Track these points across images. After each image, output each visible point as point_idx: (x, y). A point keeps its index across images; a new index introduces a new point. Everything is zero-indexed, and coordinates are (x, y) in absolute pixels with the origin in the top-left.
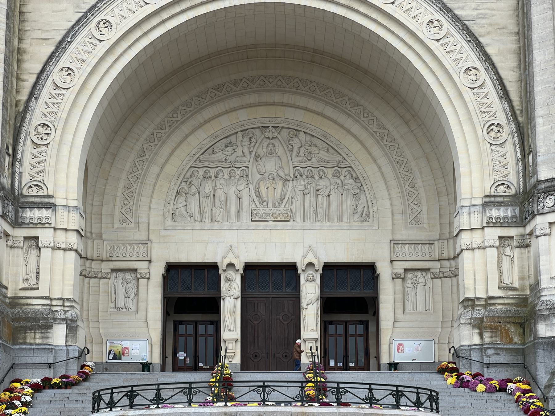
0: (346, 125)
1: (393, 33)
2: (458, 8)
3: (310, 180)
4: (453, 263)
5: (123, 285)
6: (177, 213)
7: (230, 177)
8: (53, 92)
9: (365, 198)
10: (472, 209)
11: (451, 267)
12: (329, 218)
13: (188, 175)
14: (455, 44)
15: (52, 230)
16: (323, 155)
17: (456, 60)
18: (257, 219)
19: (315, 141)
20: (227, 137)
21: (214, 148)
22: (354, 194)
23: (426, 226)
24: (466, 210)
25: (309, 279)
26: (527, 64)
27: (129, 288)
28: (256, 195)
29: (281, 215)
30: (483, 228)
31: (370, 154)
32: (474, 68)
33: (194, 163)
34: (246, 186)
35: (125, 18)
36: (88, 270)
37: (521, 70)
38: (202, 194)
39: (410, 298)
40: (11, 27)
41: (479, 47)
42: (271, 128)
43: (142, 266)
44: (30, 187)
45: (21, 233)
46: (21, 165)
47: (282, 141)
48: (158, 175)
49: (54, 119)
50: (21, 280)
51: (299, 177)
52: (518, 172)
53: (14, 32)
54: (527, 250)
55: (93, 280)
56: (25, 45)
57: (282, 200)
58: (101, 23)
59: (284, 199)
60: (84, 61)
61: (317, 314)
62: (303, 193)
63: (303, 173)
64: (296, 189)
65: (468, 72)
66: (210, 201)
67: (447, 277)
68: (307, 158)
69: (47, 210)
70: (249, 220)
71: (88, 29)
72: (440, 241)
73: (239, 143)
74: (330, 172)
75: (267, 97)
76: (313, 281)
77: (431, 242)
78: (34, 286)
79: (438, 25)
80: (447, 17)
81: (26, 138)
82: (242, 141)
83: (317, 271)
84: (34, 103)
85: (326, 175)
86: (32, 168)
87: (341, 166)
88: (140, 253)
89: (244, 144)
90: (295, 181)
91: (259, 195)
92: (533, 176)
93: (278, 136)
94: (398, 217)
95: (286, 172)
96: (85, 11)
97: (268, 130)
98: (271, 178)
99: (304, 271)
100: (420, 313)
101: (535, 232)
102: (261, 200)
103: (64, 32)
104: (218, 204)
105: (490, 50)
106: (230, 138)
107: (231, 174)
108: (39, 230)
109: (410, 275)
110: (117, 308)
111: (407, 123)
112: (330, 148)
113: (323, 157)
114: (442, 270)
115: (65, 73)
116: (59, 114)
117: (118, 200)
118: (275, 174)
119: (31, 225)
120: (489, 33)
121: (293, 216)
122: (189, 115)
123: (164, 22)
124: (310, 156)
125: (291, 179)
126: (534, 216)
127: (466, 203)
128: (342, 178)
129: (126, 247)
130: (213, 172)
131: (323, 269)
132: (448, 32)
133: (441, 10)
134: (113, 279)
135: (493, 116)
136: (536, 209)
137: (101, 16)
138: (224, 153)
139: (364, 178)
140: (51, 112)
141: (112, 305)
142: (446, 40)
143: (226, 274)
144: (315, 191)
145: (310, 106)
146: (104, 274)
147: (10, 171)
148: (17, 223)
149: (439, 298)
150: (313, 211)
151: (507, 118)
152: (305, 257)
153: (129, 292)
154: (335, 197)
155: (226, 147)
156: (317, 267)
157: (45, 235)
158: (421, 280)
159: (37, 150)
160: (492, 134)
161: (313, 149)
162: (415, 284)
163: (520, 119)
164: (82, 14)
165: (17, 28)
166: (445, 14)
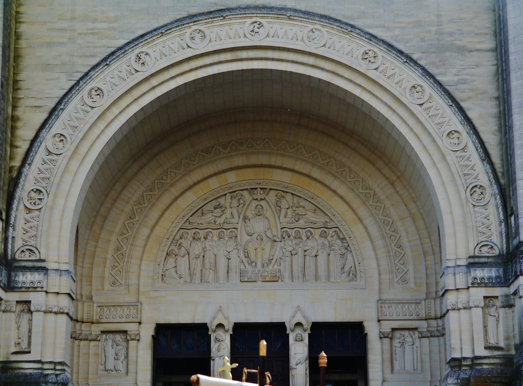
0: (333, 187)
1: (377, 97)
2: (440, 74)
3: (297, 241)
4: (440, 321)
5: (113, 347)
6: (167, 275)
7: (220, 238)
8: (46, 158)
9: (352, 258)
10: (457, 270)
11: (438, 326)
12: (317, 278)
13: (178, 237)
14: (437, 109)
15: (44, 293)
16: (311, 216)
17: (439, 124)
18: (246, 279)
19: (303, 203)
20: (215, 199)
21: (204, 210)
22: (341, 255)
23: (412, 285)
24: (451, 270)
25: (297, 339)
26: (507, 128)
27: (119, 350)
28: (245, 256)
29: (270, 275)
30: (468, 288)
31: (356, 215)
32: (456, 131)
33: (184, 225)
34: (235, 247)
35: (116, 85)
36: (78, 332)
37: (501, 134)
38: (192, 256)
39: (398, 358)
40: (5, 96)
41: (461, 110)
42: (259, 190)
43: (131, 328)
44: (23, 251)
45: (13, 297)
46: (14, 230)
47: (270, 203)
48: (148, 237)
49: (46, 185)
50: (13, 344)
51: (286, 237)
52: (501, 233)
53: (8, 100)
54: (511, 310)
55: (83, 343)
56: (19, 112)
57: (270, 260)
58: (93, 91)
59: (272, 260)
60: (76, 128)
61: (306, 374)
62: (291, 254)
63: (290, 234)
64: (284, 250)
65: (451, 135)
66: (199, 262)
67: (434, 336)
68: (295, 220)
69: (39, 275)
70: (238, 281)
71: (80, 96)
72: (427, 301)
73: (228, 205)
74: (317, 232)
75: (254, 160)
76: (302, 340)
77: (418, 302)
78: (26, 350)
79: (421, 90)
80: (429, 83)
81: (19, 203)
82: (231, 203)
83: (305, 330)
84: (27, 168)
85: (313, 235)
86: (25, 232)
87: (328, 227)
88: (130, 315)
89: (233, 205)
90: (283, 242)
91: (247, 256)
92: (515, 237)
93: (266, 198)
94: (385, 277)
95: (275, 233)
96: (77, 79)
97: (256, 192)
98: (259, 240)
99: (292, 331)
100: (408, 373)
101: (519, 292)
102: (250, 261)
103: (56, 100)
104: (207, 266)
105: (471, 114)
106: (218, 200)
107: (220, 235)
108: (31, 293)
109: (397, 334)
110: (107, 370)
111: (392, 184)
112: (317, 209)
113: (310, 218)
114: (430, 329)
115: (57, 139)
116: (52, 179)
117: (108, 261)
118: (264, 235)
119: (23, 289)
120: (470, 98)
121: (281, 276)
122: (178, 178)
123: (153, 88)
124: (298, 217)
125: (279, 240)
126: (517, 277)
127: (451, 264)
128: (329, 238)
129: (116, 309)
130: (202, 233)
131: (312, 329)
132: (431, 97)
133: (423, 76)
134: (103, 341)
135: (476, 178)
136: (519, 270)
138: (213, 214)
139: (351, 238)
140: (43, 178)
141: (102, 367)
143: (215, 334)
144: (303, 251)
145: (297, 168)
146: (94, 336)
147: (4, 236)
148: (10, 287)
149: (427, 358)
150: (301, 271)
151: (490, 180)
152: (293, 316)
153: (119, 354)
154: (322, 258)
155: (215, 208)
156: (305, 327)
158: (409, 339)
159: (29, 215)
160: (476, 196)
161: (300, 211)
162: (403, 344)
163: (502, 181)
164: (76, 82)
165: (11, 96)
166: (427, 79)
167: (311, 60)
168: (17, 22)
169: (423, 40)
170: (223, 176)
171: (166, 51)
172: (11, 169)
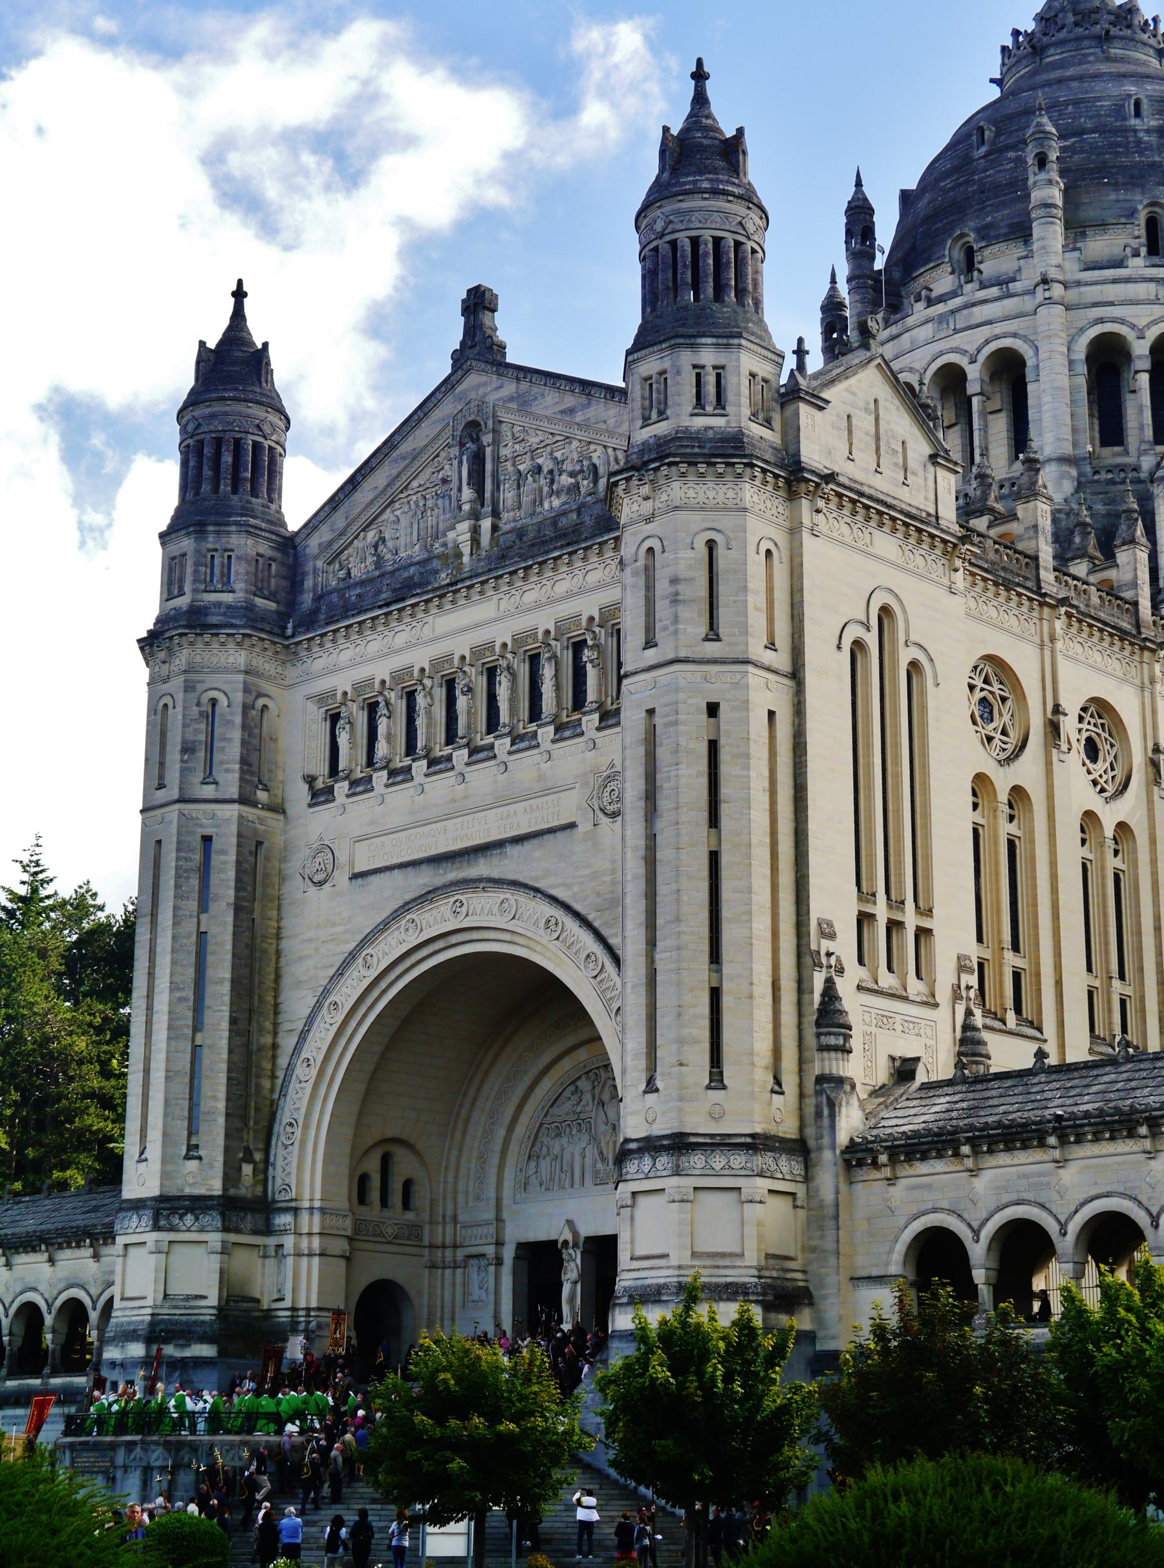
45: (272, 1241)
56: (279, 1040)
104: (565, 1168)
123: (384, 992)
132: (603, 966)
137: (332, 998)
142: (603, 976)
157: (289, 1241)
167: (507, 937)
168: (278, 937)
169: (598, 894)
170: (574, 1055)
171: (386, 949)
172: (272, 1101)
